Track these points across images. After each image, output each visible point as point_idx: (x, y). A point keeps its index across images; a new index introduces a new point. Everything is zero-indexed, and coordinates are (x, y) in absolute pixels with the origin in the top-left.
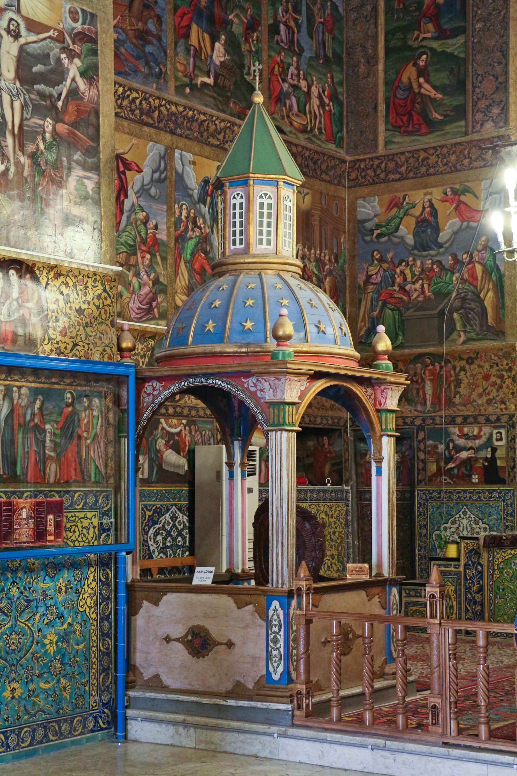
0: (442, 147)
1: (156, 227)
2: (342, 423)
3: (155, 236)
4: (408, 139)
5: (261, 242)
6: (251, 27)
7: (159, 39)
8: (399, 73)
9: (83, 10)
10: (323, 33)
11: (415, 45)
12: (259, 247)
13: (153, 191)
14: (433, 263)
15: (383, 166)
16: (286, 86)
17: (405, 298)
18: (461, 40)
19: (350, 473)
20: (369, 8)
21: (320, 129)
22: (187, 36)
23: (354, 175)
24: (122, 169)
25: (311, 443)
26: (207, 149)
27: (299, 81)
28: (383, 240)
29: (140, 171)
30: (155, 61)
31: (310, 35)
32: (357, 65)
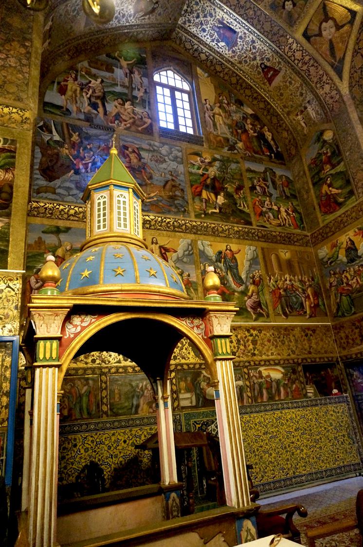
0: (347, 211)
1: (189, 275)
2: (335, 359)
3: (188, 280)
4: (331, 215)
5: (99, 227)
6: (240, 188)
7: (183, 198)
8: (320, 191)
9: (4, 139)
10: (283, 187)
11: (324, 176)
12: (97, 231)
13: (185, 260)
14: (359, 267)
15: (324, 231)
16: (264, 209)
17: (350, 288)
18: (342, 163)
19: (346, 386)
20: (302, 173)
21: (289, 225)
22: (200, 194)
23: (313, 241)
24: (163, 252)
25: (323, 373)
26: (218, 239)
27: (272, 206)
28: (333, 264)
29: (175, 252)
30: (182, 206)
31: (275, 189)
32: (303, 196)
